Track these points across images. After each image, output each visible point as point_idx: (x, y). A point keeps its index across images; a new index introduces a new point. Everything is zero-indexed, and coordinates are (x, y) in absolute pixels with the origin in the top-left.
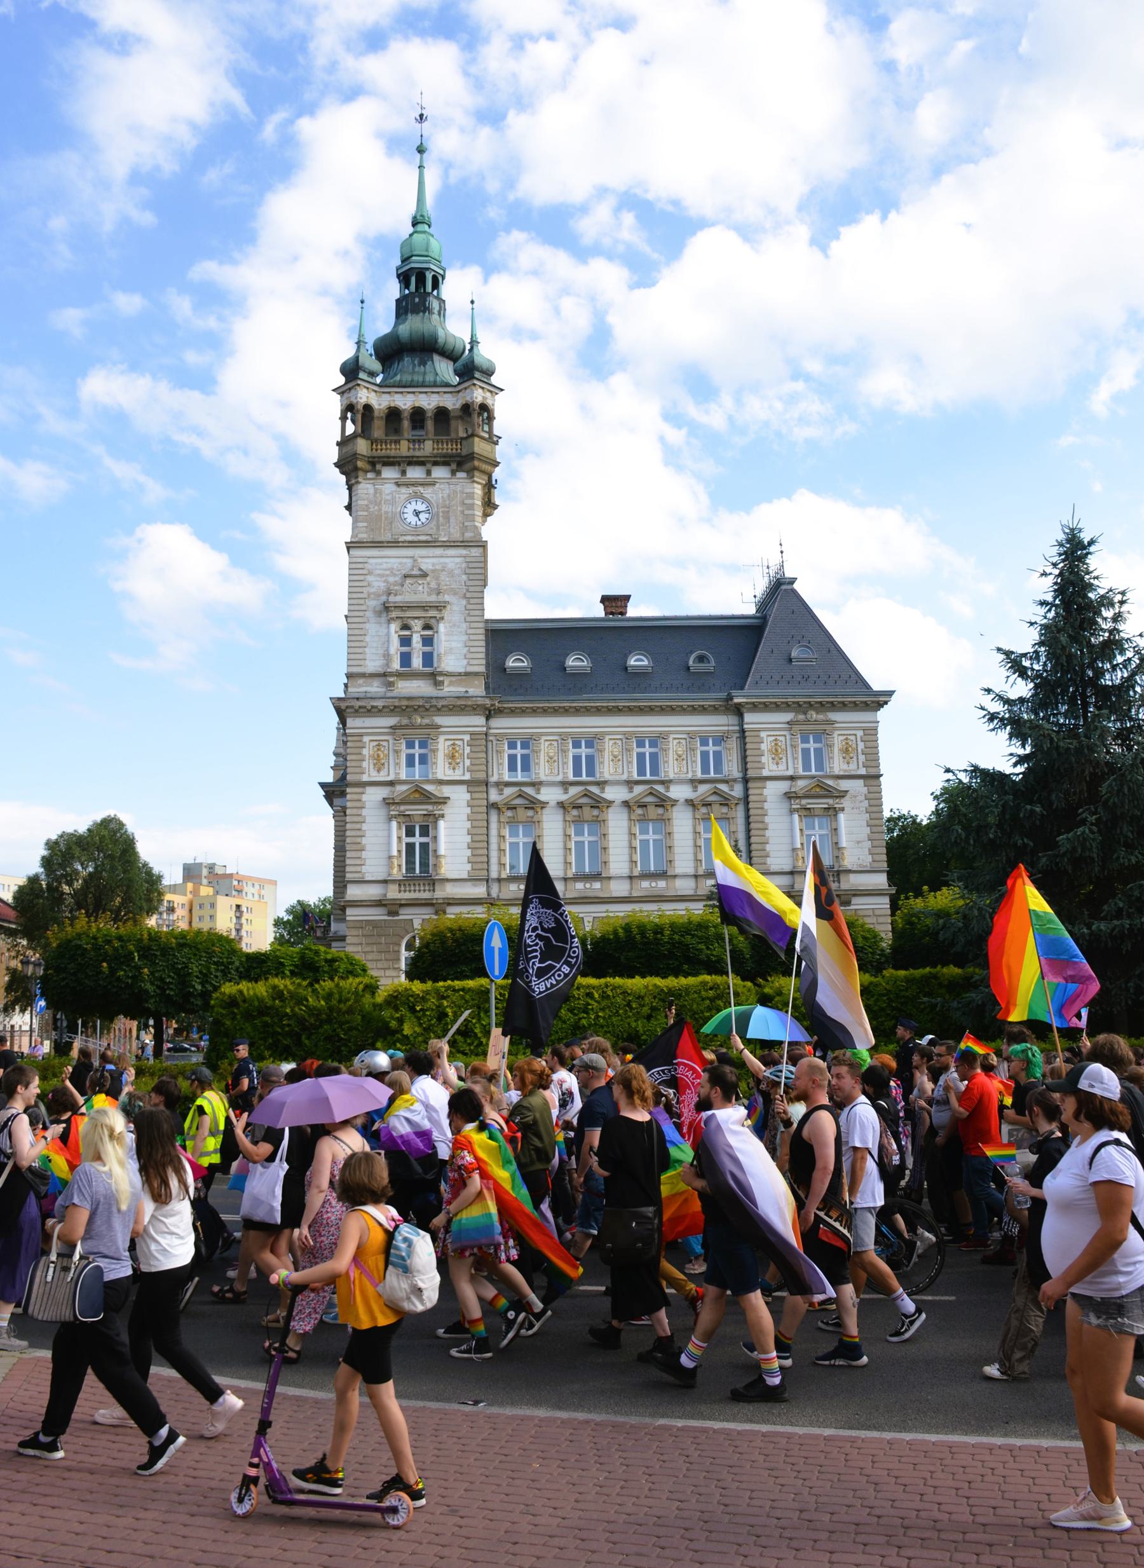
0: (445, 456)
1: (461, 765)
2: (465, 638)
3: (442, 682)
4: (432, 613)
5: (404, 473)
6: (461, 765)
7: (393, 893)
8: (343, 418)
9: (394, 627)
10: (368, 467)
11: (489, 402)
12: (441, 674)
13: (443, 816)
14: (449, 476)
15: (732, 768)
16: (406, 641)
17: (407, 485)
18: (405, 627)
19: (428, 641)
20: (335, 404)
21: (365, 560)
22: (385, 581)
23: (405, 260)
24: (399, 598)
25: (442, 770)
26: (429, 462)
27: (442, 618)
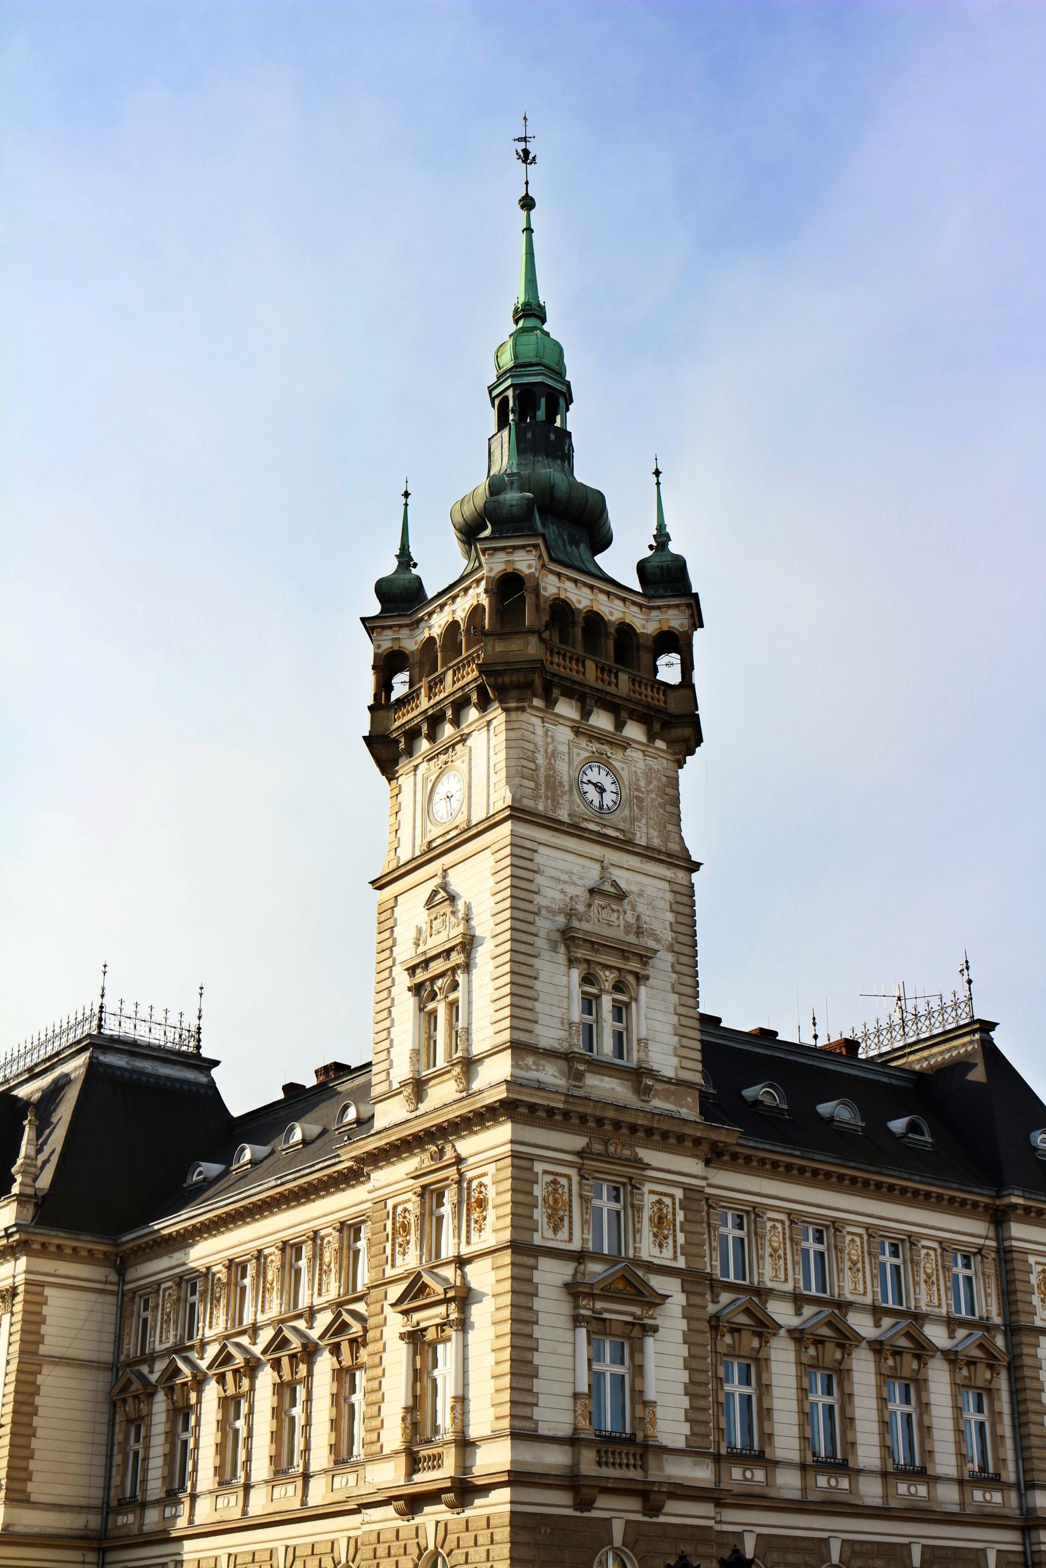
0: (649, 707)
1: (670, 1240)
2: (675, 1019)
4: (634, 965)
5: (586, 714)
6: (670, 1240)
7: (588, 1464)
9: (576, 974)
12: (651, 1073)
13: (655, 1329)
14: (644, 740)
15: (989, 1306)
16: (589, 1003)
19: (620, 1011)
21: (535, 846)
22: (562, 892)
24: (585, 926)
25: (647, 1249)
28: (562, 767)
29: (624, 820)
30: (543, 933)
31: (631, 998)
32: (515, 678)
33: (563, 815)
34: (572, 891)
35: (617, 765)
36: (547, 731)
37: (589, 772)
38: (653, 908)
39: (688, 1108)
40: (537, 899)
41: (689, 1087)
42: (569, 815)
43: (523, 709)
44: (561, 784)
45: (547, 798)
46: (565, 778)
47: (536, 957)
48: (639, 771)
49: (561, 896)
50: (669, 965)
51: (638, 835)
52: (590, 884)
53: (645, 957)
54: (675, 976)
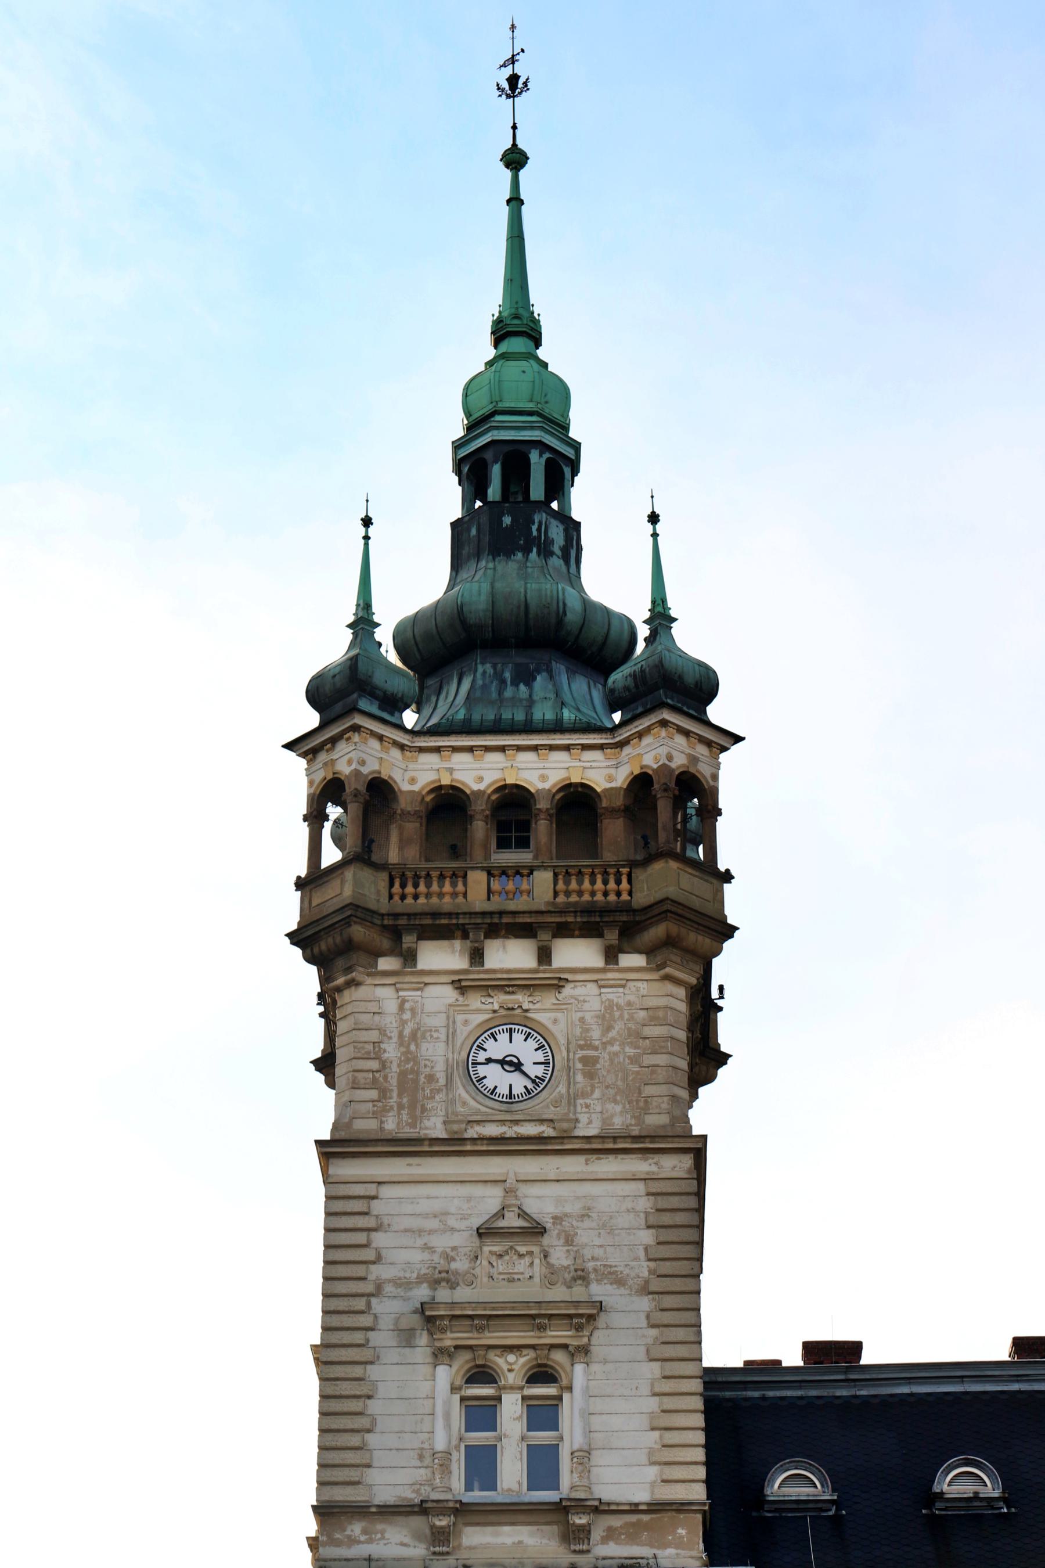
0: (589, 910)
2: (653, 1404)
3: (585, 1532)
5: (477, 956)
8: (315, 817)
9: (445, 1375)
10: (386, 943)
11: (704, 769)
14: (599, 962)
16: (482, 1415)
17: (488, 988)
18: (482, 1375)
19: (543, 1415)
20: (294, 780)
21: (371, 1190)
22: (426, 1247)
23: (475, 426)
24: (463, 1294)
26: (544, 926)
27: (585, 1350)
28: (436, 1054)
29: (556, 1104)
30: (386, 1323)
31: (562, 1388)
32: (330, 940)
33: (435, 1127)
34: (442, 1242)
35: (543, 1018)
36: (403, 1002)
37: (490, 1044)
38: (611, 1232)
39: (679, 1544)
40: (376, 1272)
41: (679, 1511)
42: (445, 1122)
43: (353, 983)
44: (431, 1078)
45: (401, 1107)
46: (440, 1067)
47: (372, 1363)
48: (588, 1017)
49: (426, 1256)
50: (643, 1316)
51: (583, 1118)
52: (477, 1222)
53: (586, 1317)
54: (654, 1332)
